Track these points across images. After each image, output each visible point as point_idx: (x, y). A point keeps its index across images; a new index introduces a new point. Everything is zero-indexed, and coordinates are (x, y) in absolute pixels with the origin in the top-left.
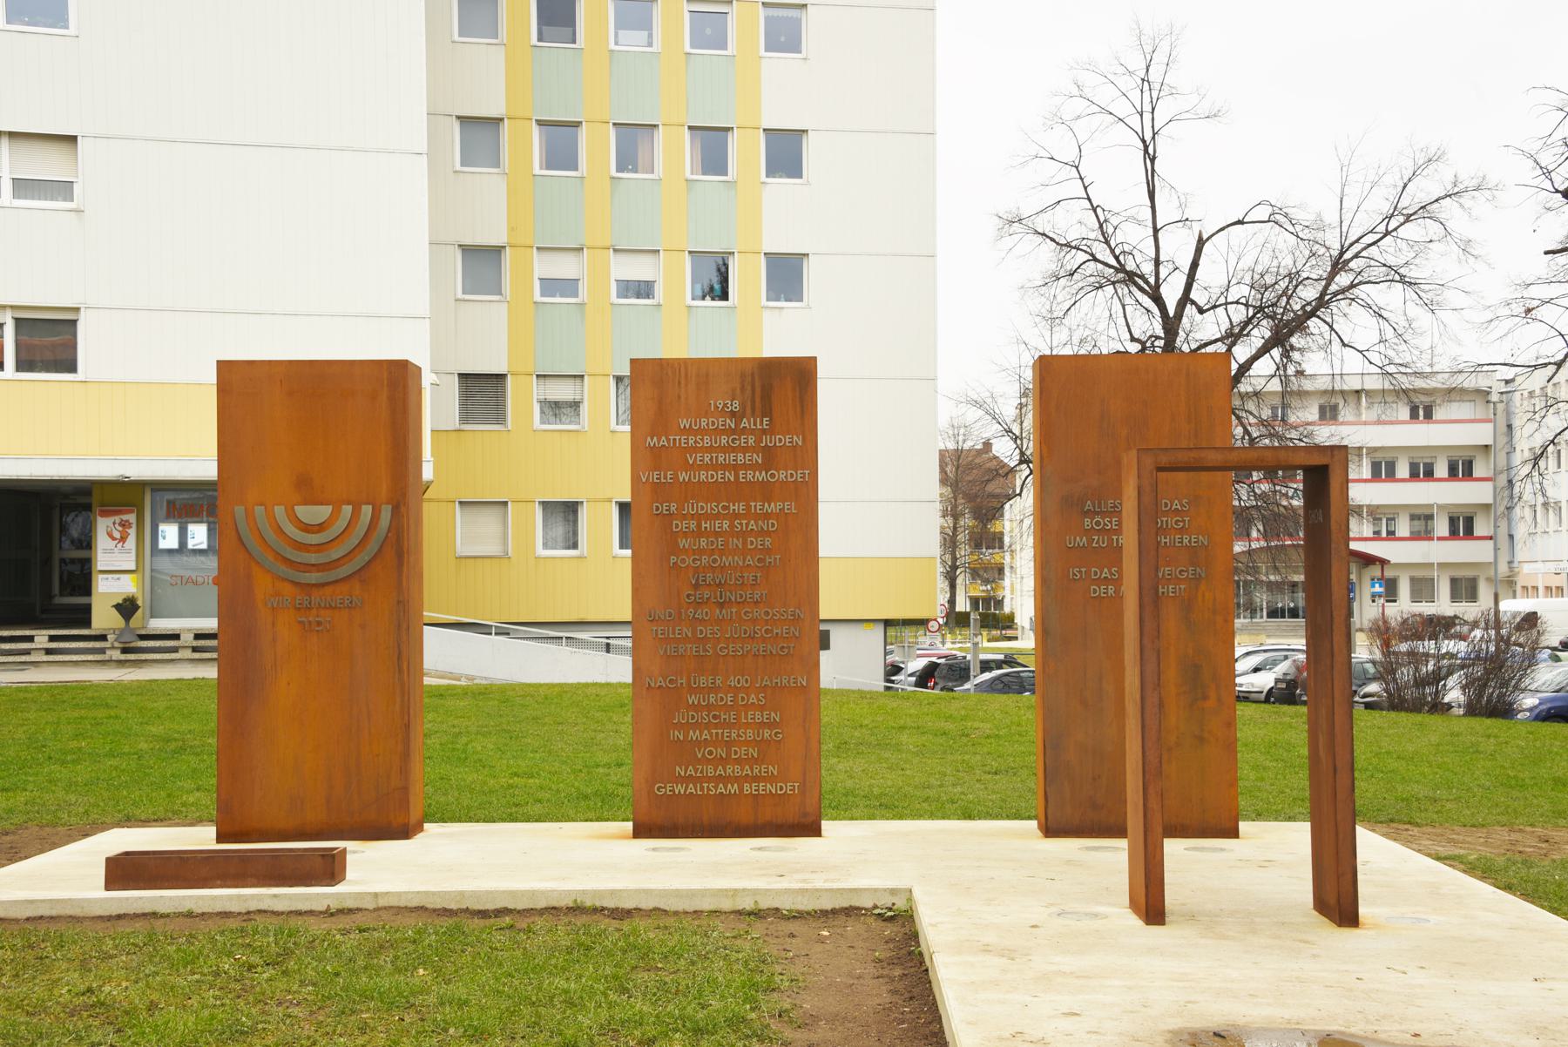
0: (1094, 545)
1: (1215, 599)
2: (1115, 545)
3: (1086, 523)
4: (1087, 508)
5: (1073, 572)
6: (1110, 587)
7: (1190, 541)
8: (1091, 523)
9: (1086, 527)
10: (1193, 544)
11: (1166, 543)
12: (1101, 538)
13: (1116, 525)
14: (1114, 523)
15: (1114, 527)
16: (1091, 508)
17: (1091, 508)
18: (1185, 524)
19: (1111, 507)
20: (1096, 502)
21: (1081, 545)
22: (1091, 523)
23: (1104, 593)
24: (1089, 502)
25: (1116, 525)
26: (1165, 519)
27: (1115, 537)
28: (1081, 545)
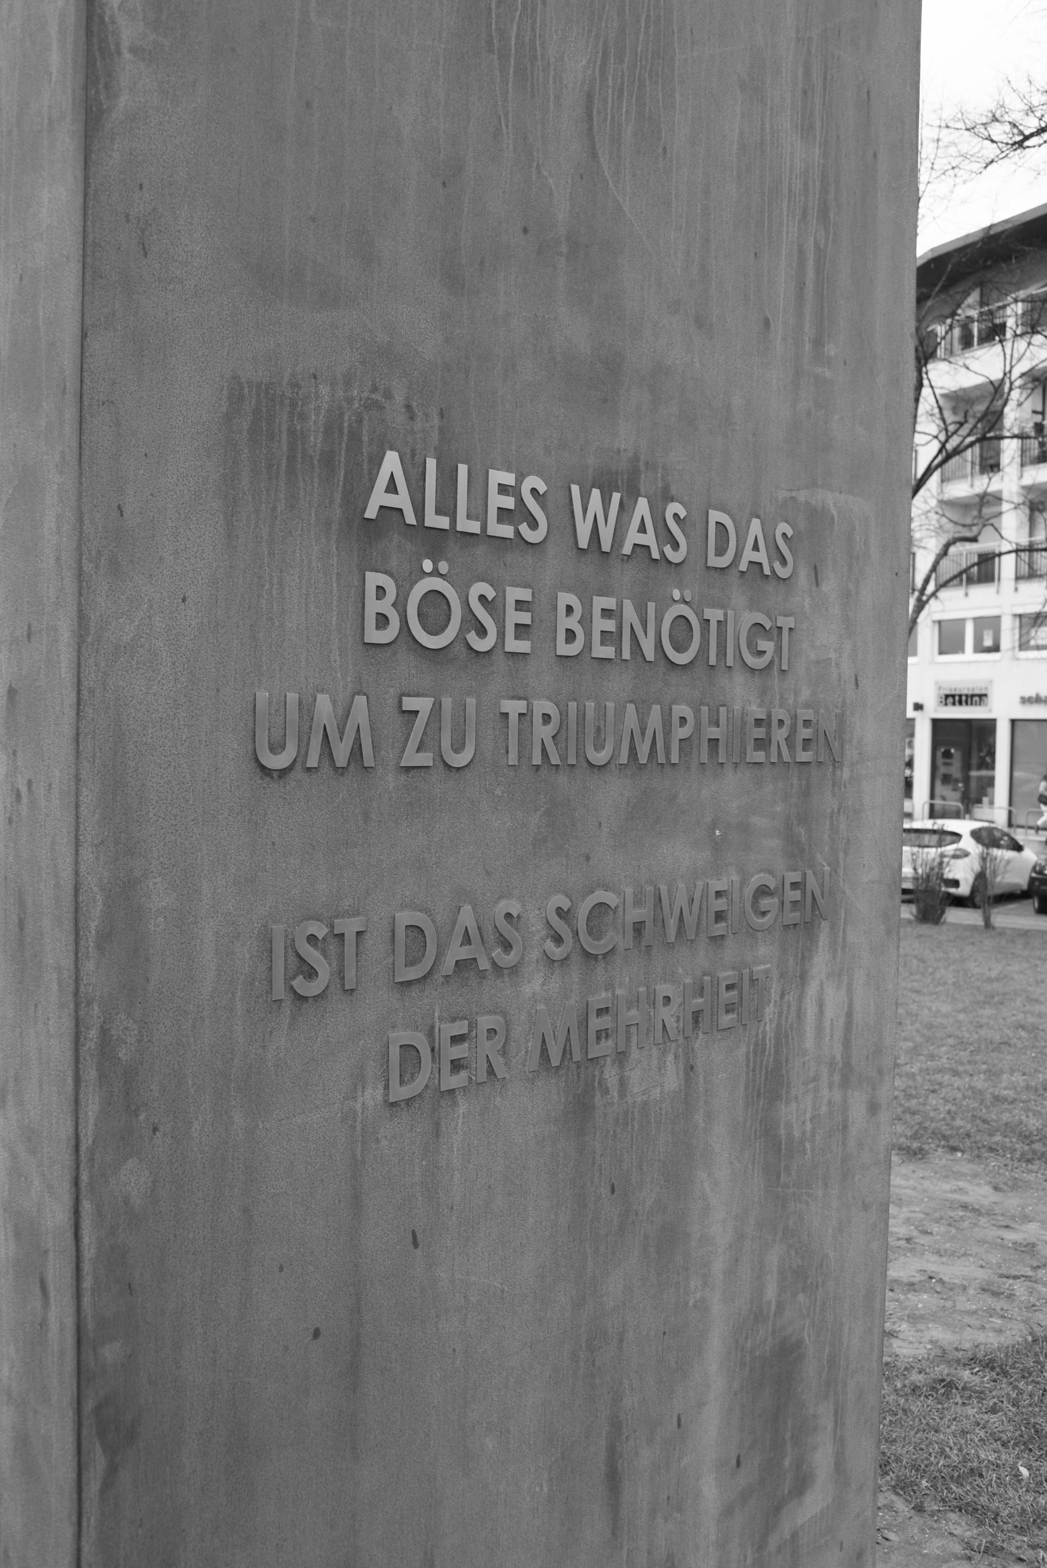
0: (412, 758)
1: (849, 1015)
2: (513, 759)
3: (373, 606)
4: (379, 498)
5: (291, 946)
6: (485, 1022)
7: (790, 740)
8: (400, 605)
9: (374, 636)
10: (804, 756)
11: (714, 742)
12: (447, 702)
13: (522, 630)
14: (514, 617)
15: (513, 645)
16: (402, 500)
17: (402, 500)
18: (779, 648)
19: (504, 514)
20: (431, 464)
21: (342, 753)
22: (400, 605)
23: (457, 1066)
24: (391, 463)
25: (522, 630)
26: (714, 615)
27: (514, 707)
28: (342, 753)
